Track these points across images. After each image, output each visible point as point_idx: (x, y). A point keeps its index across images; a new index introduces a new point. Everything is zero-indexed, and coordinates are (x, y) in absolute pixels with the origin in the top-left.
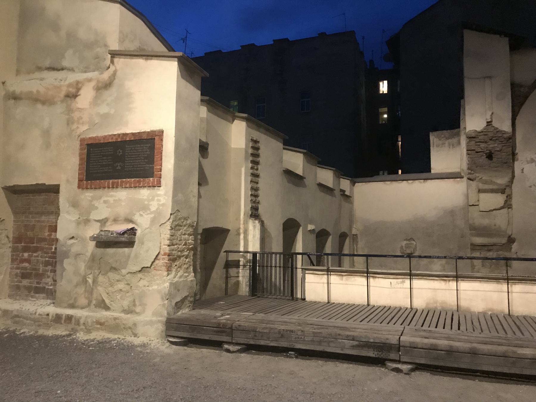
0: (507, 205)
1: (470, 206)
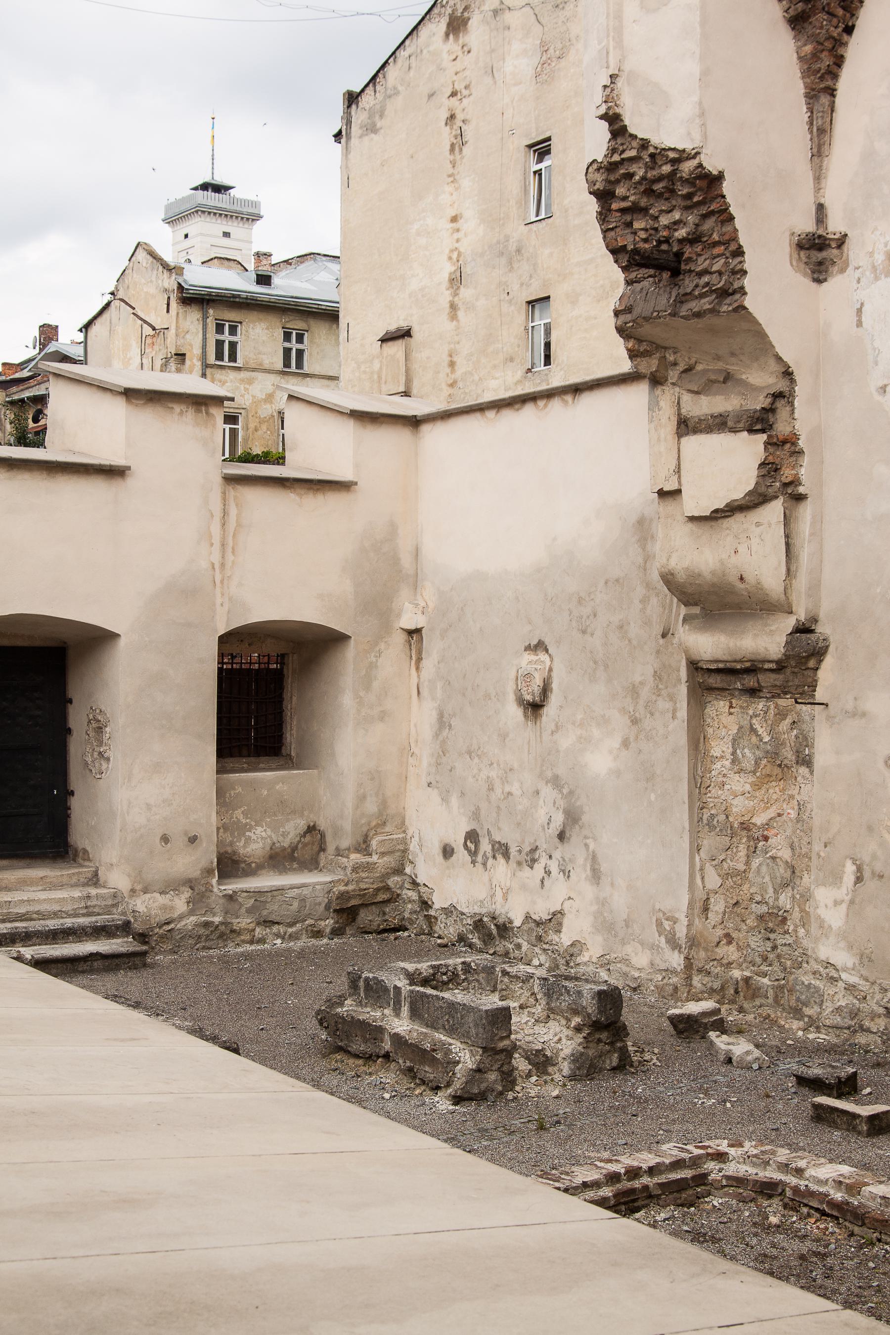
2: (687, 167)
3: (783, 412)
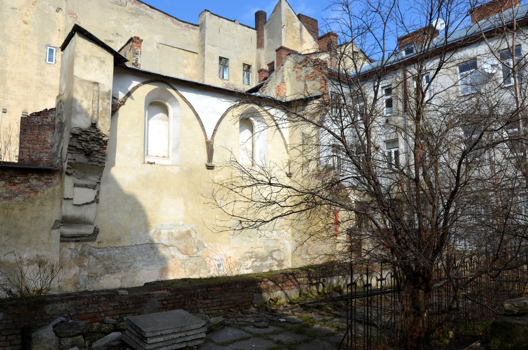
0: (96, 200)
1: (65, 199)
2: (105, 139)
3: (98, 186)
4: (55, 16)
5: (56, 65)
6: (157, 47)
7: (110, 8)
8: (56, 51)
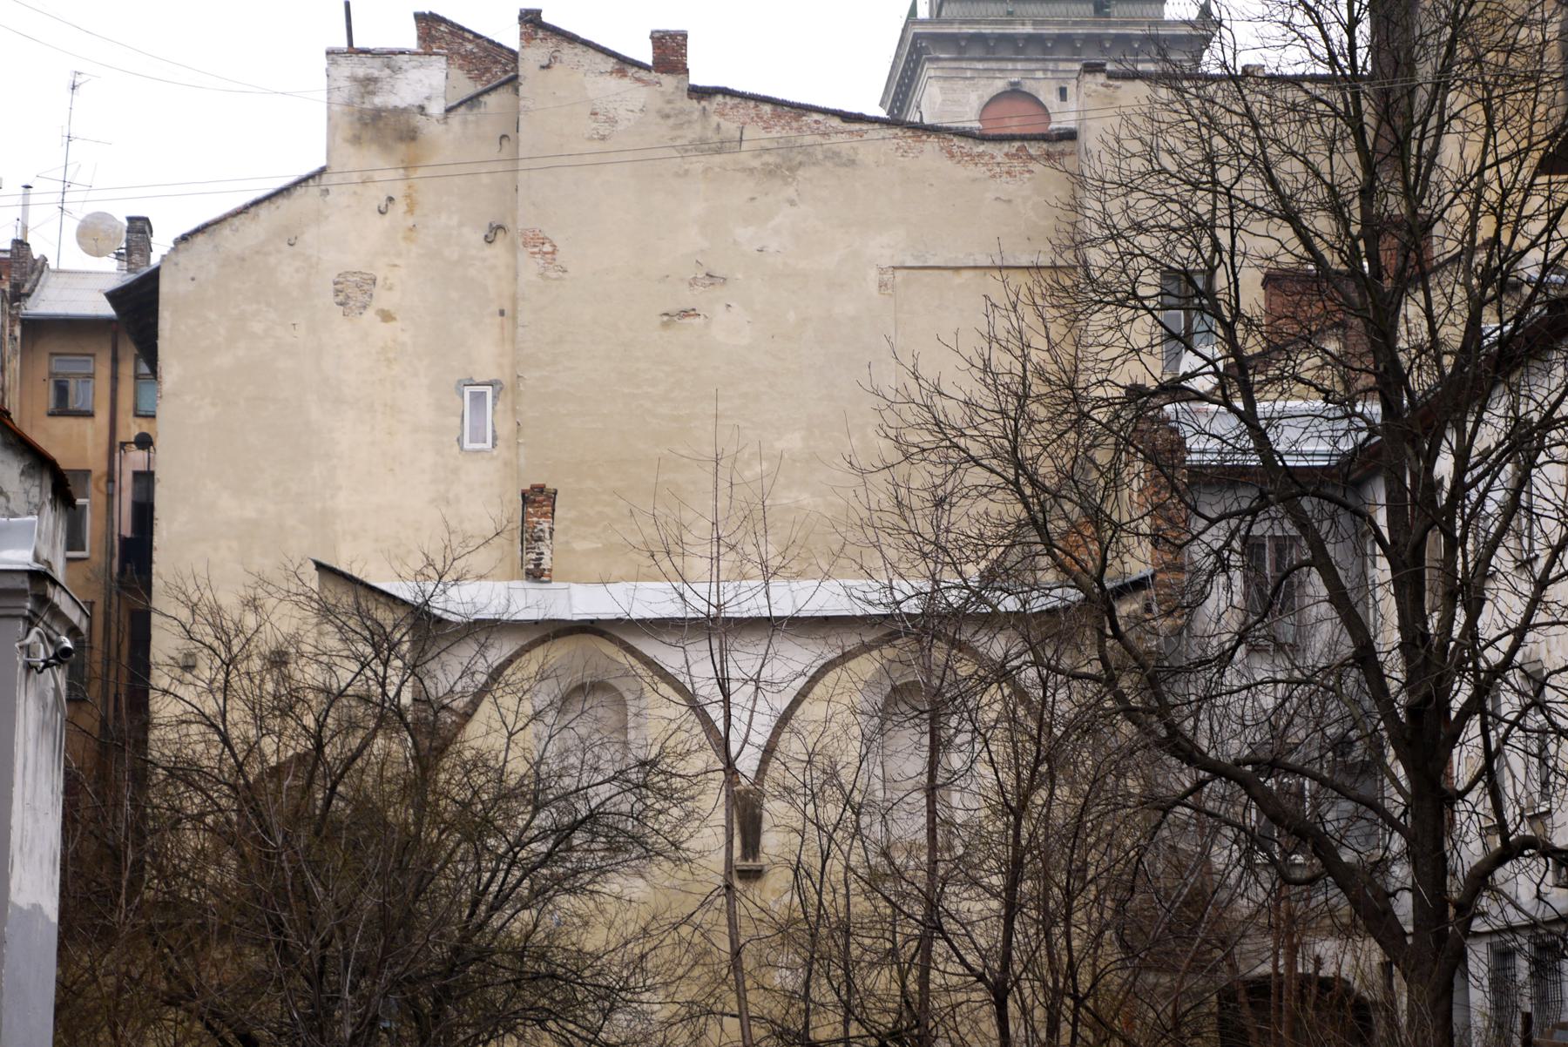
4: (484, 260)
5: (495, 453)
6: (882, 285)
7: (677, 175)
8: (495, 398)
